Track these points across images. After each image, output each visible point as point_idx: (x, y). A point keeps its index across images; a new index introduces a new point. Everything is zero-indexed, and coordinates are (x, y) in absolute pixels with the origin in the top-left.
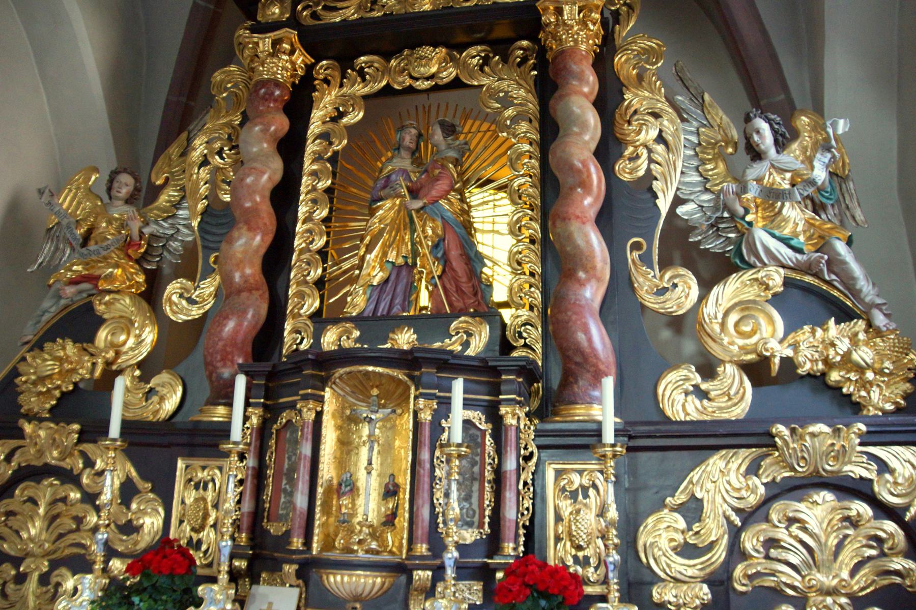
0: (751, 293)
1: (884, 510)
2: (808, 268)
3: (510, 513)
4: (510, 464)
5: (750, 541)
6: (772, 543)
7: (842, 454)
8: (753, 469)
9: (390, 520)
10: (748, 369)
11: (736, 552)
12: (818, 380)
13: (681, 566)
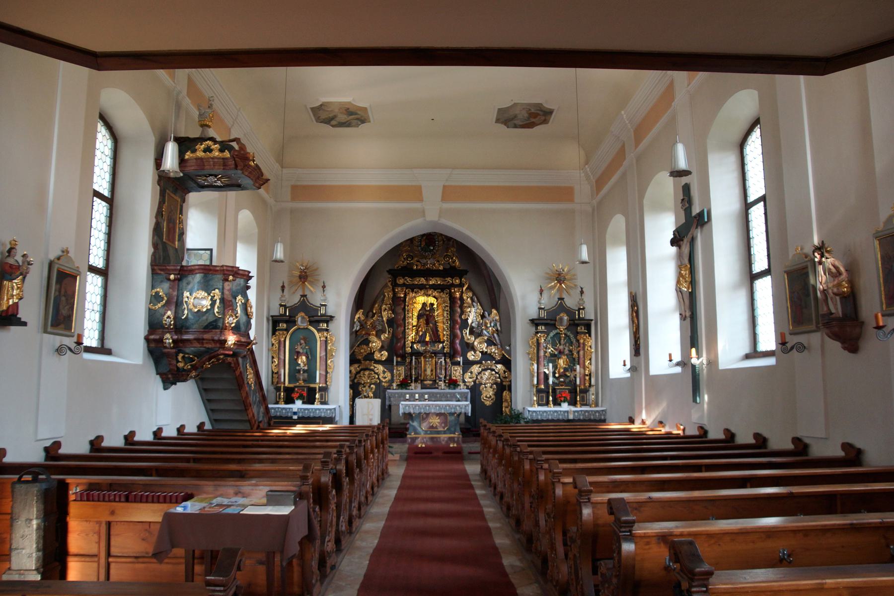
0: (481, 341)
1: (496, 373)
2: (491, 337)
3: (448, 373)
4: (447, 367)
5: (479, 377)
6: (482, 377)
7: (491, 366)
8: (480, 367)
9: (432, 375)
10: (480, 352)
11: (477, 378)
12: (490, 354)
13: (471, 380)
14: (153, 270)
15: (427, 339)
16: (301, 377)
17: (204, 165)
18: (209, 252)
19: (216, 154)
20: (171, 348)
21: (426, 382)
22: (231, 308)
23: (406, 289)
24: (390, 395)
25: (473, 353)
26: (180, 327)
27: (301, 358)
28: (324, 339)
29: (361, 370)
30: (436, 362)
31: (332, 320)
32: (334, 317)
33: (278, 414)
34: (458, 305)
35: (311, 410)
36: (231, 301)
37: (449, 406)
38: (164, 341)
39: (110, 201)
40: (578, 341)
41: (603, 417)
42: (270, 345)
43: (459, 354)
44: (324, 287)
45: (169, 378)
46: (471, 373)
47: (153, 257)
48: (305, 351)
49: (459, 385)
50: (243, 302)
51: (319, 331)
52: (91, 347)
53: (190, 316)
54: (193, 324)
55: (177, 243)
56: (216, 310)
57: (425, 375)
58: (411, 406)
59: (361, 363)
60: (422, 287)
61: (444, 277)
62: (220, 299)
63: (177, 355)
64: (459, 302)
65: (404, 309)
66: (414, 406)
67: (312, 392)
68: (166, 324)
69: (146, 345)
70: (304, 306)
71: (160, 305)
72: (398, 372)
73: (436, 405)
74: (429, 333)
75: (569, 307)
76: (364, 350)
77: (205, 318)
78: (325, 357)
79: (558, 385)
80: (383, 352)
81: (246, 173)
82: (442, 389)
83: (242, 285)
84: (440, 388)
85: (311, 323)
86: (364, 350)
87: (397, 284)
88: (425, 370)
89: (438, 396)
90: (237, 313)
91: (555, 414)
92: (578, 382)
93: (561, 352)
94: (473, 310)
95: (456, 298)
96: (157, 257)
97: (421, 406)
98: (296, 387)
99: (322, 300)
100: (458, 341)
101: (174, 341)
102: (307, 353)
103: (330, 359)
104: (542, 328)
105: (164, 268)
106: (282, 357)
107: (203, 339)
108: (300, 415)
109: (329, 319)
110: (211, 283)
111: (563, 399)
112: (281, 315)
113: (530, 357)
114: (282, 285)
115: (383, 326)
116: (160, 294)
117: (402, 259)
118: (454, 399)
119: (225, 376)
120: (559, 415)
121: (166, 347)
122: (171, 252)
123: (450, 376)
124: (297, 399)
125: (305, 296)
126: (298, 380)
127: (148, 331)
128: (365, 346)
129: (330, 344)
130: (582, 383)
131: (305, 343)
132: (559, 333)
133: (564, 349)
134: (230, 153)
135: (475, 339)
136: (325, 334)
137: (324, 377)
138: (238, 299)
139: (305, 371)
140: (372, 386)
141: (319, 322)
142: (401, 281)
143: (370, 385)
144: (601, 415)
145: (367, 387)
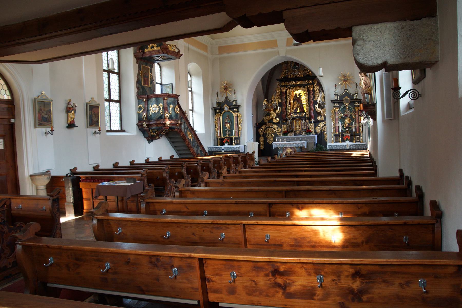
3: (307, 127)
4: (307, 124)
9: (299, 128)
13: (319, 130)
14: (138, 98)
15: (298, 111)
16: (228, 134)
17: (151, 54)
18: (171, 85)
19: (155, 48)
20: (146, 128)
21: (296, 132)
22: (167, 110)
23: (286, 87)
24: (278, 139)
25: (320, 117)
26: (149, 119)
27: (227, 125)
28: (236, 116)
29: (267, 128)
30: (301, 122)
31: (240, 107)
32: (240, 106)
33: (217, 150)
34: (311, 94)
35: (230, 148)
36: (167, 107)
37: (295, 143)
38: (144, 125)
39: (119, 74)
40: (355, 110)
41: (365, 148)
42: (214, 120)
43: (313, 118)
44: (235, 92)
45: (149, 139)
46: (319, 126)
47: (137, 93)
48: (229, 122)
49: (312, 133)
50: (173, 107)
51: (234, 112)
52: (116, 130)
53: (152, 115)
54: (153, 118)
55: (150, 85)
56: (161, 111)
57: (296, 128)
58: (278, 144)
59: (267, 124)
60: (294, 86)
61: (304, 81)
62: (162, 107)
63: (150, 131)
64: (312, 92)
65: (286, 97)
66: (279, 144)
67: (232, 139)
68: (144, 119)
69: (138, 127)
70: (227, 102)
71: (141, 112)
72: (284, 128)
73: (289, 144)
74: (299, 108)
75: (350, 93)
76: (268, 118)
77: (157, 115)
78: (237, 124)
79: (345, 132)
80: (277, 119)
81: (170, 54)
82: (303, 135)
83: (172, 100)
84: (302, 134)
85: (230, 109)
86: (268, 118)
87: (281, 85)
88: (296, 126)
89: (296, 138)
90: (170, 112)
91: (341, 146)
92: (354, 131)
93: (346, 116)
94: (320, 95)
95: (310, 90)
96: (139, 92)
97: (282, 144)
98: (225, 138)
99: (234, 98)
100: (312, 112)
101: (147, 125)
102: (229, 122)
103: (240, 124)
104: (336, 104)
105: (141, 97)
106: (219, 125)
107: (157, 124)
108: (226, 150)
109: (238, 107)
110: (159, 101)
111: (346, 139)
112: (217, 106)
113: (332, 119)
114: (217, 93)
115: (277, 106)
116: (141, 107)
117: (283, 73)
118: (298, 140)
119: (178, 136)
120: (359, 146)
121: (144, 128)
122: (147, 90)
123: (309, 128)
124: (225, 143)
125: (227, 97)
126: (226, 135)
127: (138, 122)
128: (268, 116)
129: (239, 118)
130: (357, 131)
131: (229, 118)
132: (346, 106)
133: (348, 114)
134: (160, 47)
135: (321, 110)
136: (236, 114)
137: (237, 133)
138: (170, 106)
139: (229, 131)
140: (273, 135)
141: (233, 108)
142: (283, 84)
143: (272, 134)
144: (364, 146)
145: (270, 135)
